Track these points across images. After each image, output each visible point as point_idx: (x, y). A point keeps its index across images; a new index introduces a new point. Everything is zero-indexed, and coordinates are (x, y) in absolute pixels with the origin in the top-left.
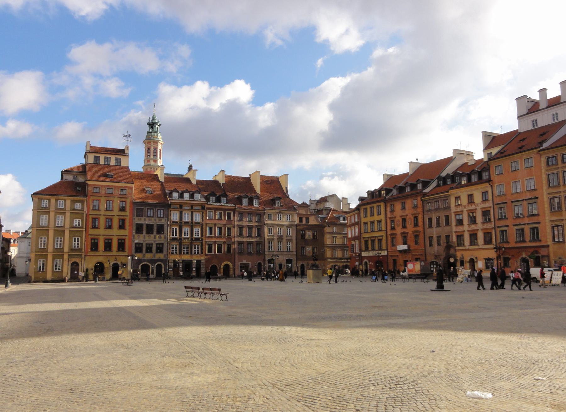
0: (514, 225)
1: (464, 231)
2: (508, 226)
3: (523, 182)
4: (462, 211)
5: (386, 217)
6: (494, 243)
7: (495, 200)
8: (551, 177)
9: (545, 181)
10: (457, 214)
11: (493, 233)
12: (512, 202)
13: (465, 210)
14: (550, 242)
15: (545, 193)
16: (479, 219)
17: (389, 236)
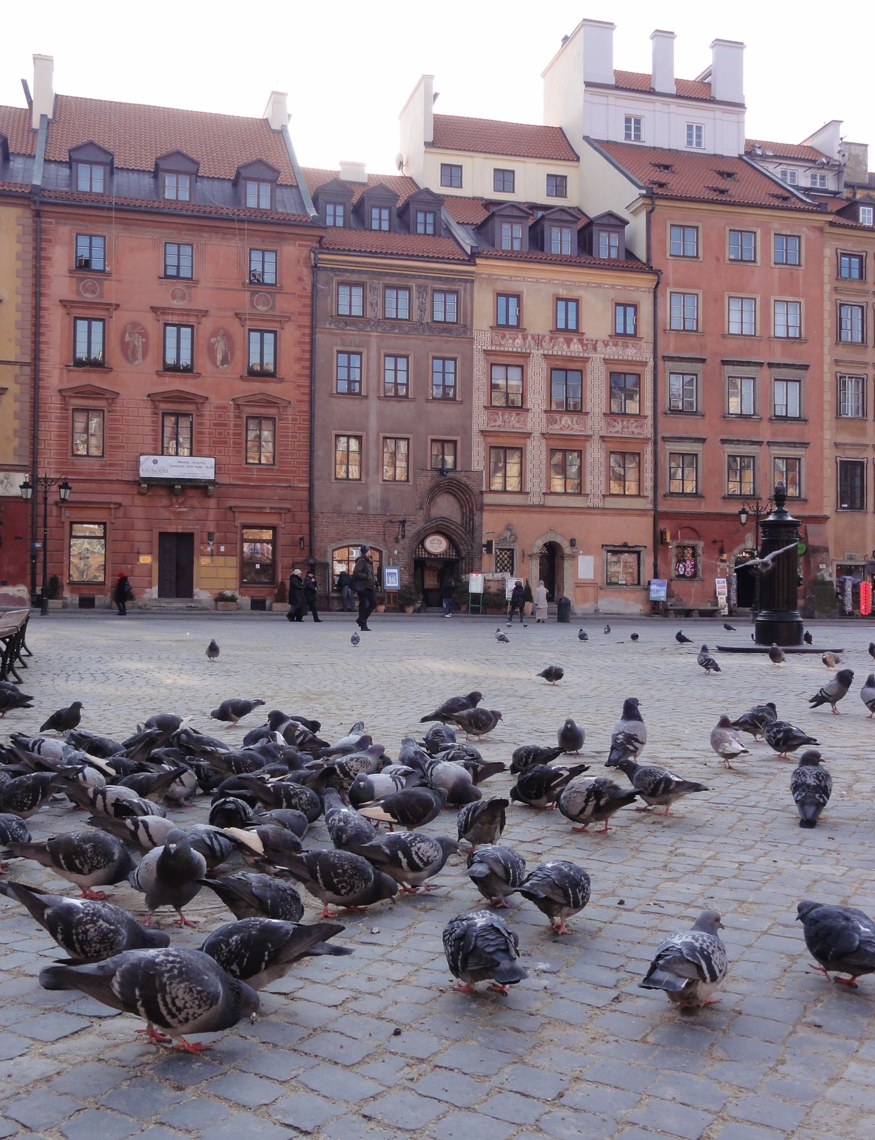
0: (723, 441)
1: (528, 435)
2: (702, 440)
3: (766, 305)
4: (526, 356)
5: (38, 294)
6: (649, 493)
7: (661, 343)
8: (846, 312)
9: (828, 323)
10: (497, 359)
11: (648, 457)
12: (724, 363)
13: (537, 353)
14: (828, 510)
15: (827, 359)
16: (596, 395)
17: (52, 403)
